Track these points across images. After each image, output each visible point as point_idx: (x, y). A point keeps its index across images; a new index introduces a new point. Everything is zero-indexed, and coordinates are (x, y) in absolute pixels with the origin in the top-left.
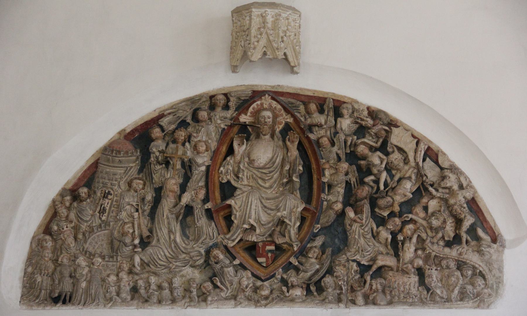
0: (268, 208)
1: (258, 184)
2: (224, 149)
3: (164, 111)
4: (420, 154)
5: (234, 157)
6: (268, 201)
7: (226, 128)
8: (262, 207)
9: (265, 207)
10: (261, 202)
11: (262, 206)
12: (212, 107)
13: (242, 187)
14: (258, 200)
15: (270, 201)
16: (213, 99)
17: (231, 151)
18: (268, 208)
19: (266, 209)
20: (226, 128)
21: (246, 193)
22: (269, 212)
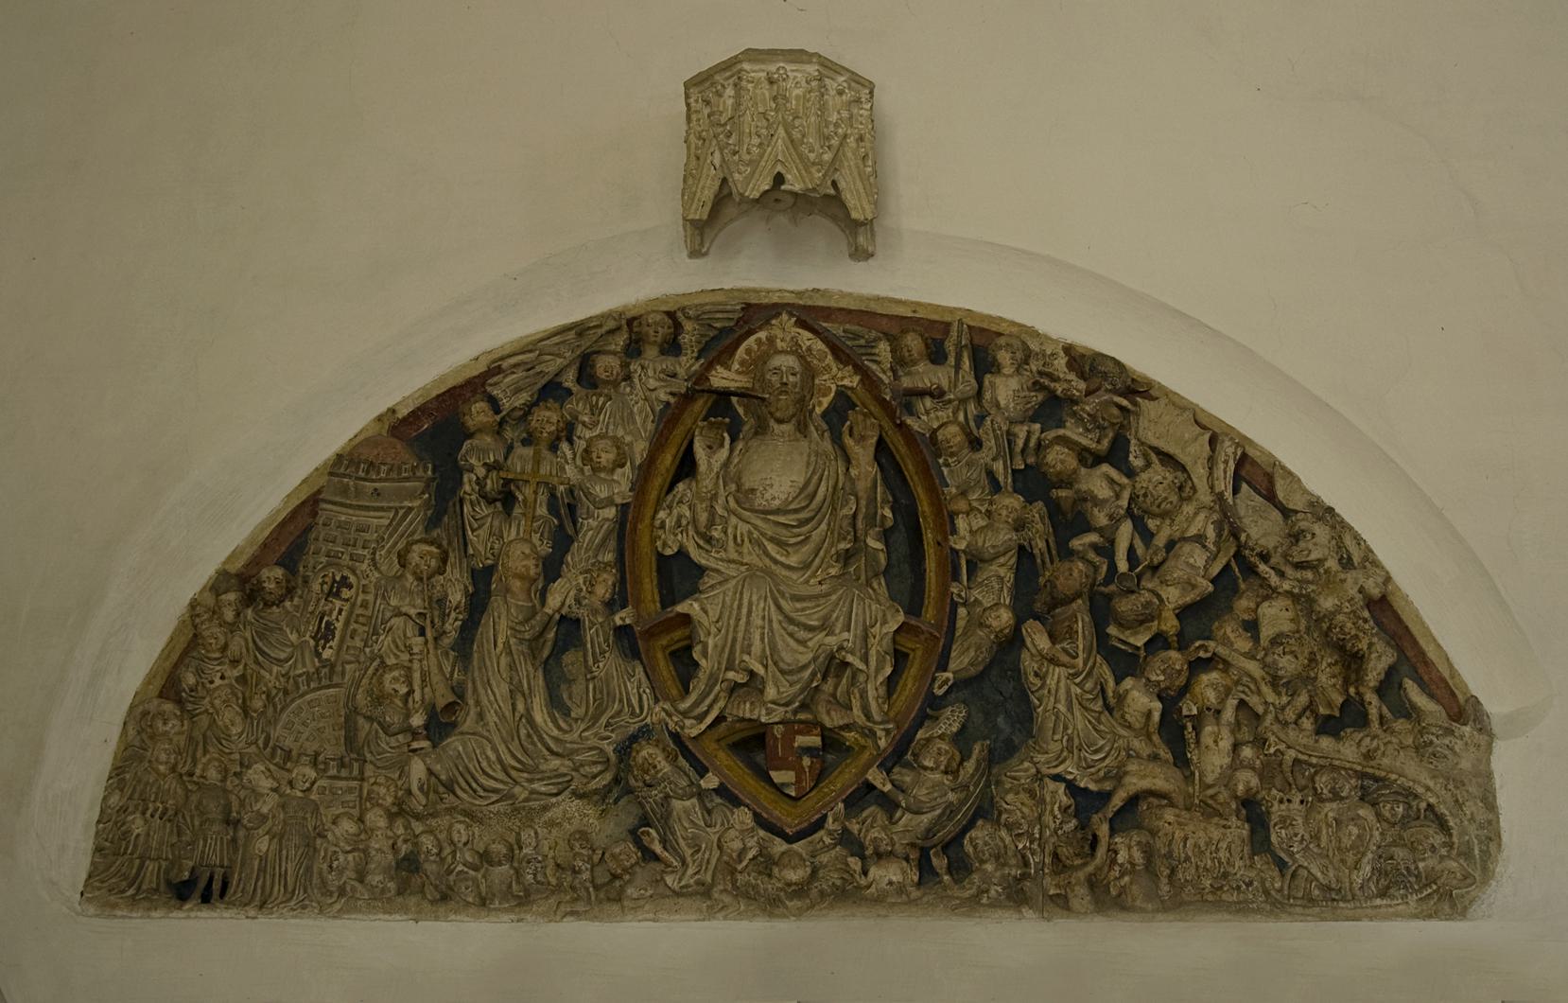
0: (798, 624)
1: (767, 554)
2: (668, 460)
3: (502, 359)
4: (1225, 472)
5: (697, 482)
6: (798, 605)
7: (672, 400)
8: (780, 622)
9: (791, 621)
10: (779, 607)
11: (781, 618)
12: (634, 349)
13: (721, 566)
14: (770, 600)
15: (805, 605)
16: (635, 323)
17: (687, 467)
18: (798, 624)
19: (791, 628)
20: (672, 400)
21: (734, 582)
22: (802, 634)
